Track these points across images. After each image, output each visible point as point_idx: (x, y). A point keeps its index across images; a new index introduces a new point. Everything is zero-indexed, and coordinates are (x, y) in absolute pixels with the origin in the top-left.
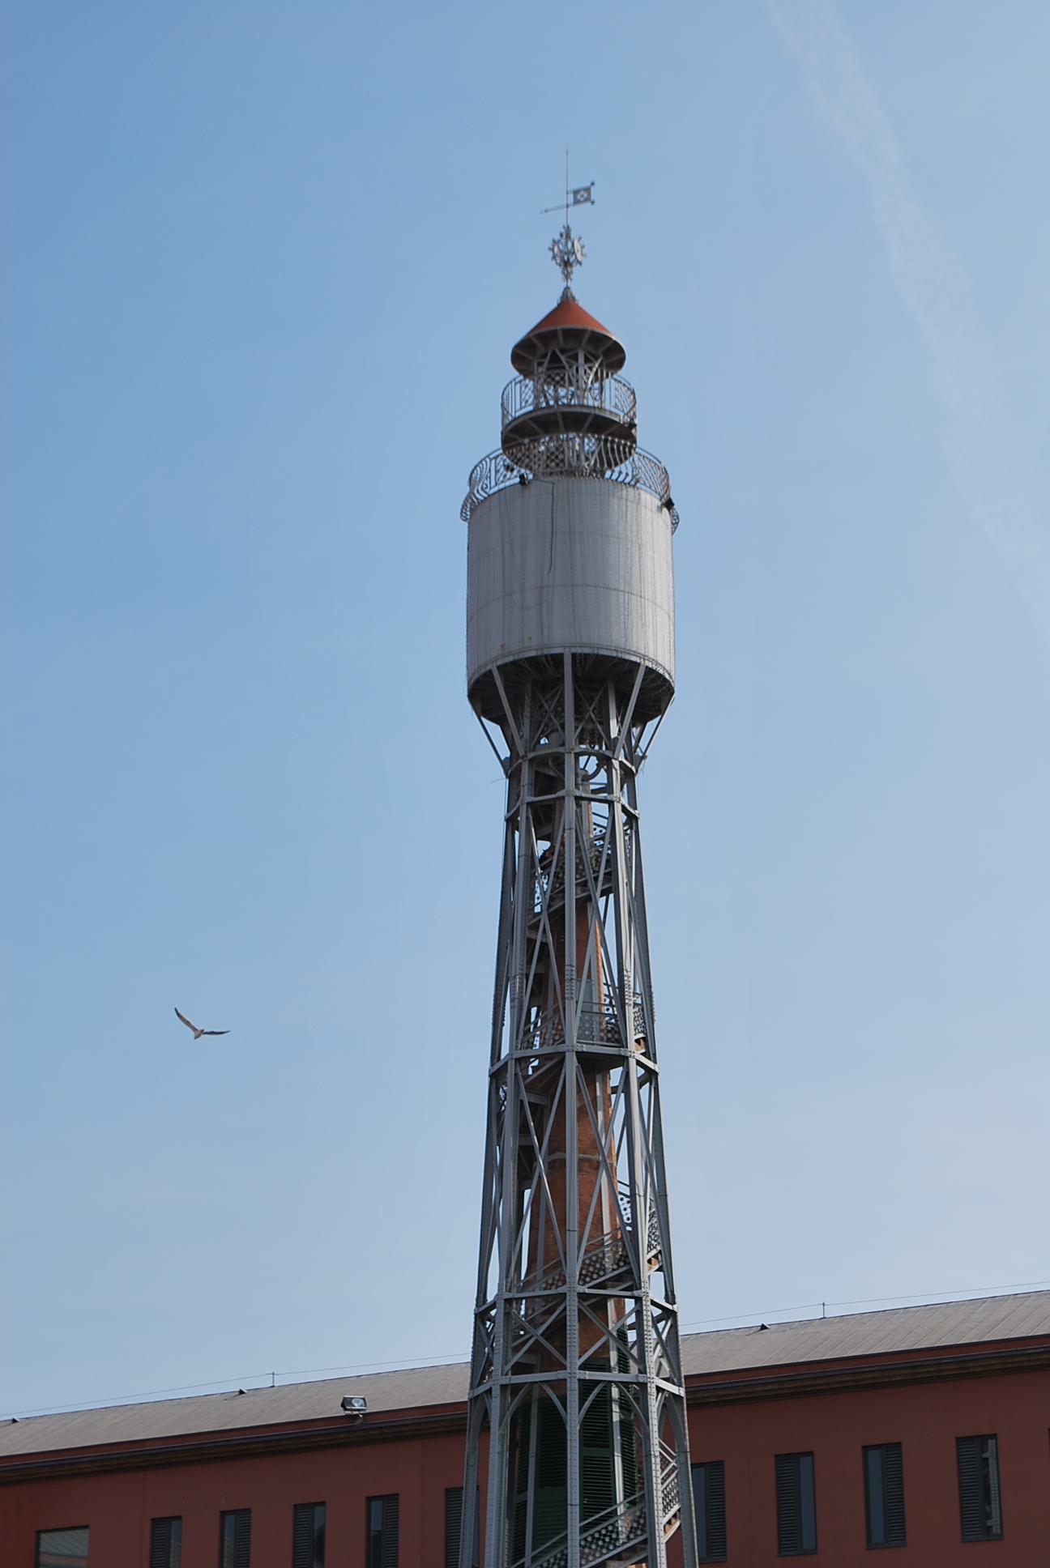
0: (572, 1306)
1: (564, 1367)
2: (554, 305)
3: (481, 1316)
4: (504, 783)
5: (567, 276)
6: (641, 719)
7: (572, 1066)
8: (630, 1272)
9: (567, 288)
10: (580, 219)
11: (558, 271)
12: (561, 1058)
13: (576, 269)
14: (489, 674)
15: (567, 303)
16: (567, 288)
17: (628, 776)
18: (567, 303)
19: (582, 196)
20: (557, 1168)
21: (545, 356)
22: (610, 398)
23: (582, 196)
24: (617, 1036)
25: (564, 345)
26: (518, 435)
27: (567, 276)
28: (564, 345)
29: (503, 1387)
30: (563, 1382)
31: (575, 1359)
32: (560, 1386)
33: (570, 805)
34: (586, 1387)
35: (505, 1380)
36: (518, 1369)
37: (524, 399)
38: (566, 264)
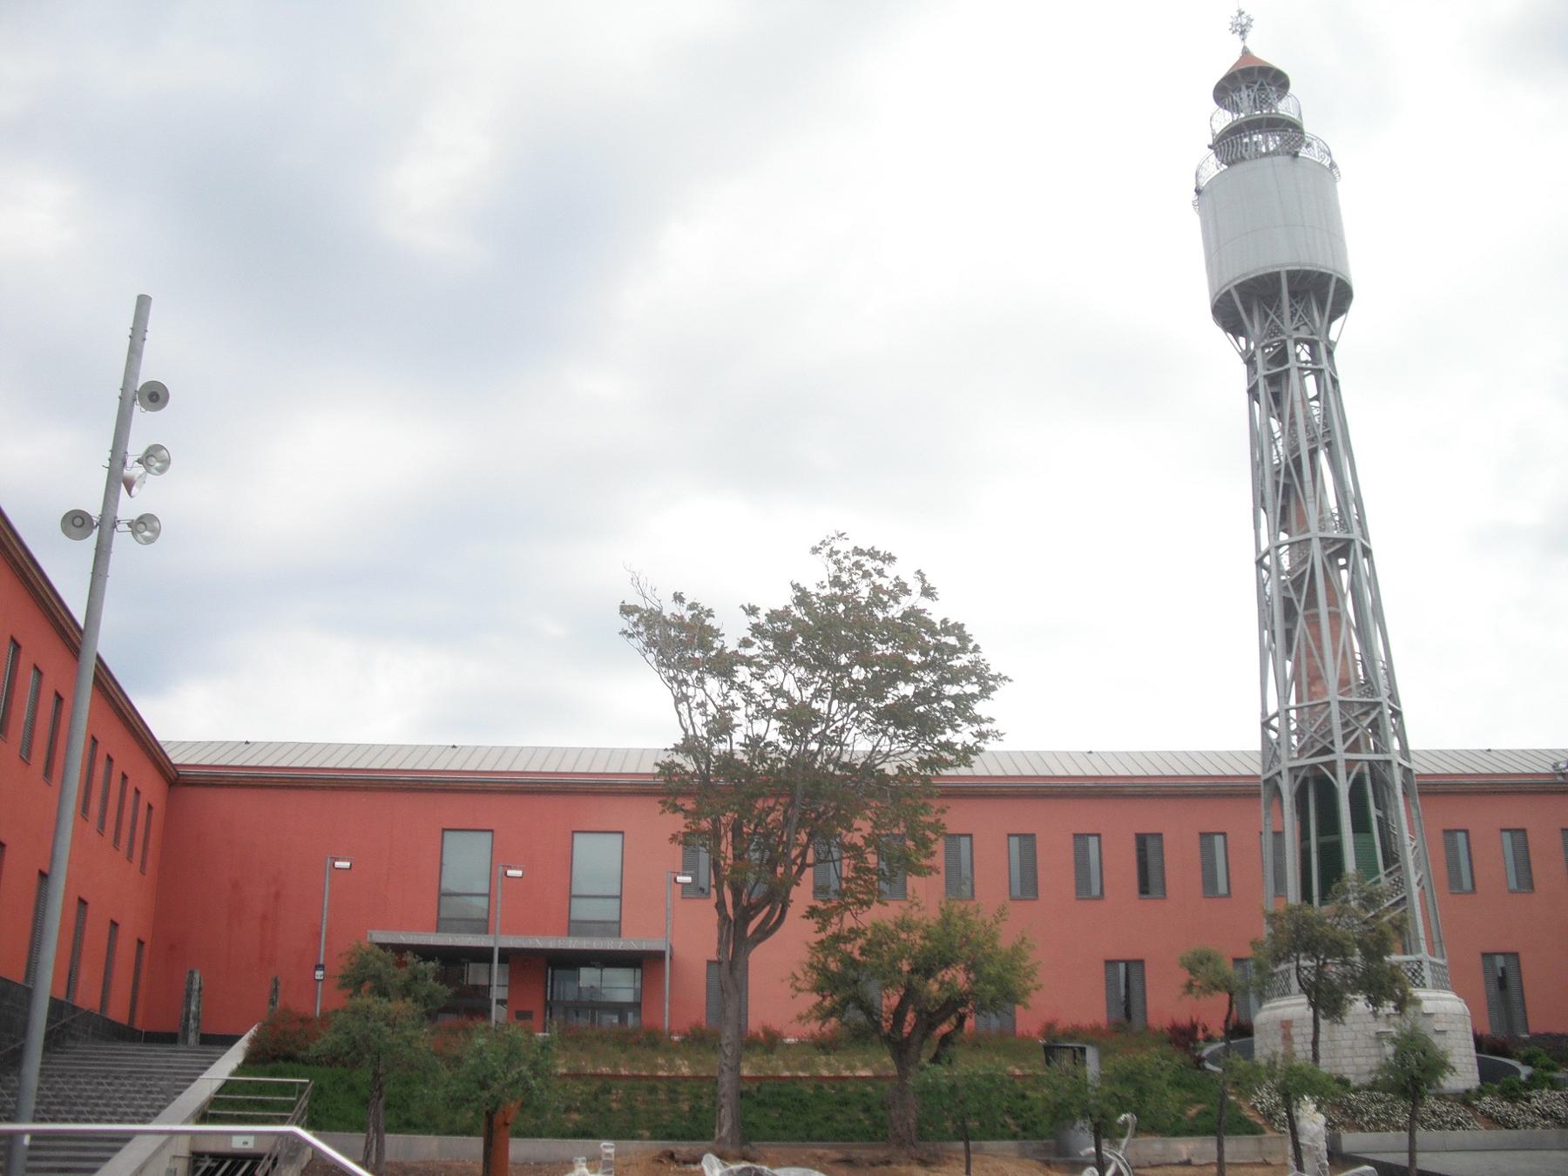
0: (1335, 709)
3: (1266, 725)
4: (1243, 368)
6: (1332, 319)
7: (1316, 546)
11: (1237, 36)
13: (1250, 35)
15: (1246, 52)
17: (1330, 353)
18: (1246, 52)
20: (1313, 621)
22: (1285, 108)
24: (1344, 525)
25: (1252, 84)
26: (1228, 145)
29: (1291, 769)
30: (1334, 762)
31: (1339, 747)
32: (1331, 765)
33: (1294, 374)
34: (1350, 764)
37: (1225, 119)
38: (1242, 33)
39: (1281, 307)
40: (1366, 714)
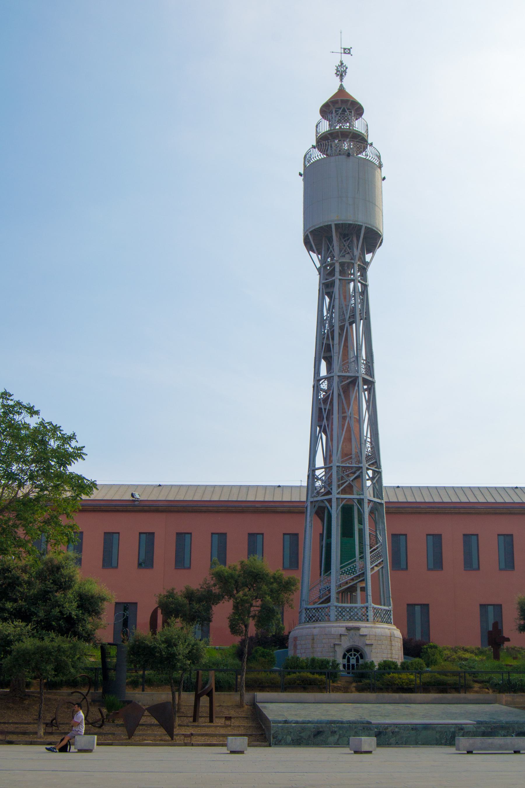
1: (331, 494)
2: (336, 91)
5: (341, 80)
8: (376, 462)
9: (341, 85)
10: (346, 59)
12: (356, 378)
13: (345, 79)
14: (330, 226)
15: (341, 90)
16: (341, 85)
18: (341, 90)
19: (347, 51)
21: (340, 108)
23: (347, 51)
25: (342, 107)
27: (341, 80)
28: (342, 107)
35: (338, 496)
36: (338, 493)
39: (342, 240)
40: (354, 473)
